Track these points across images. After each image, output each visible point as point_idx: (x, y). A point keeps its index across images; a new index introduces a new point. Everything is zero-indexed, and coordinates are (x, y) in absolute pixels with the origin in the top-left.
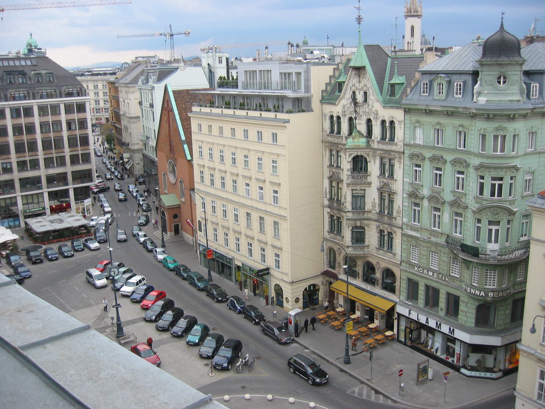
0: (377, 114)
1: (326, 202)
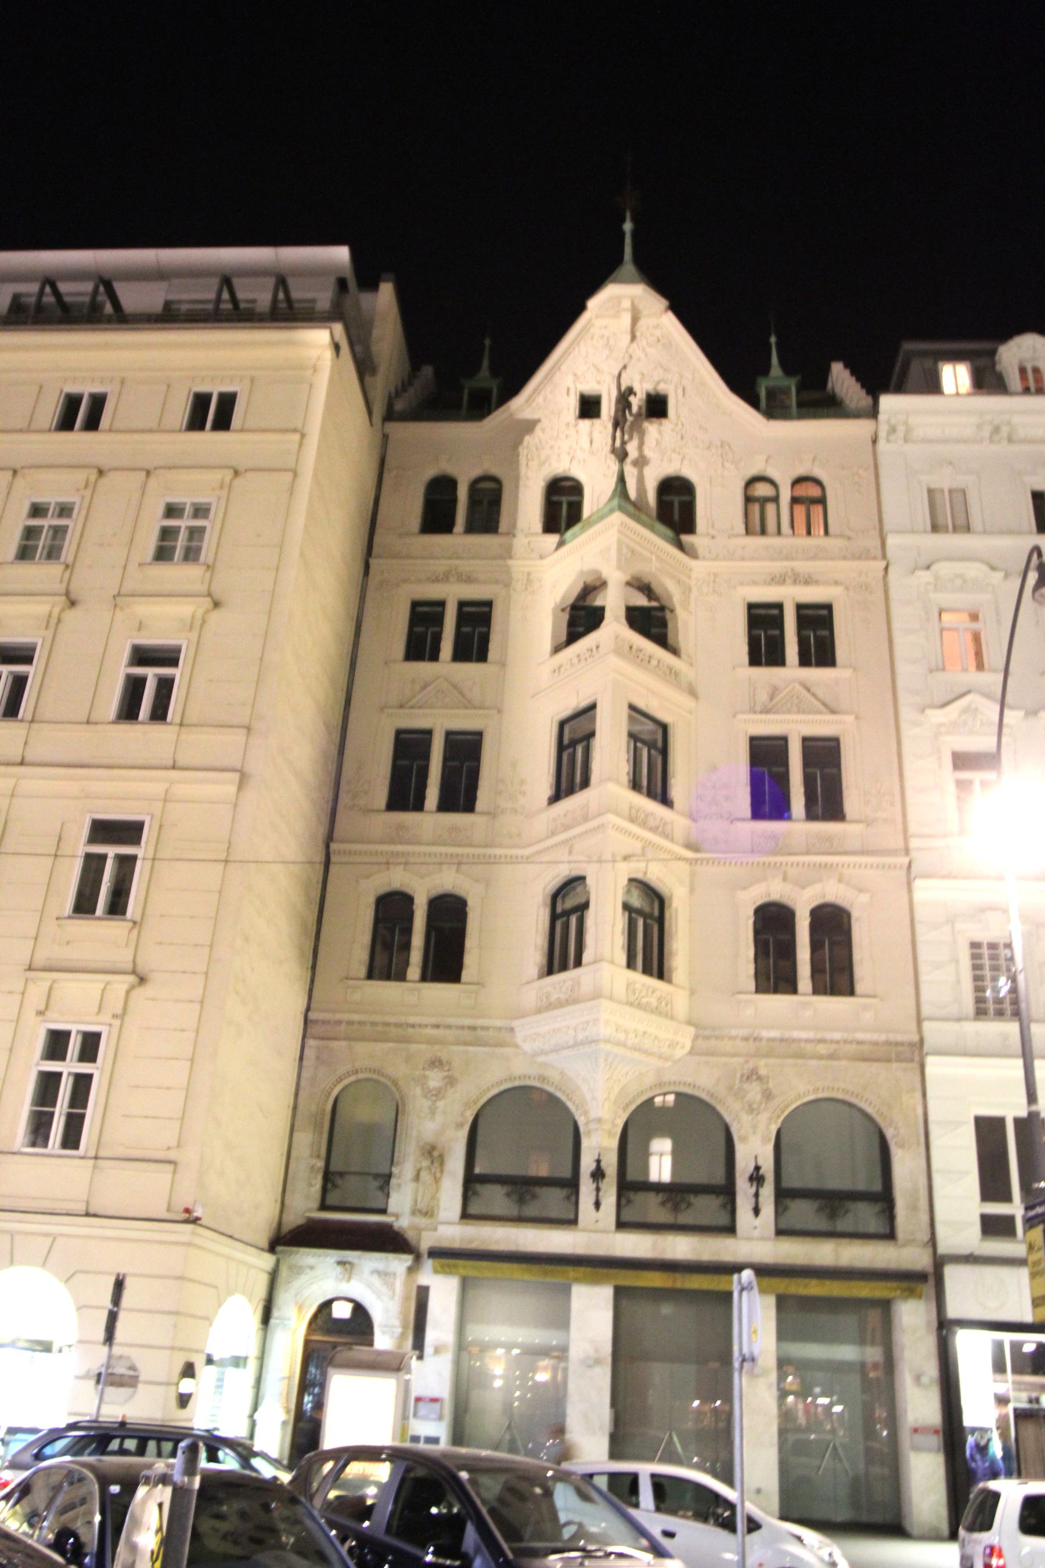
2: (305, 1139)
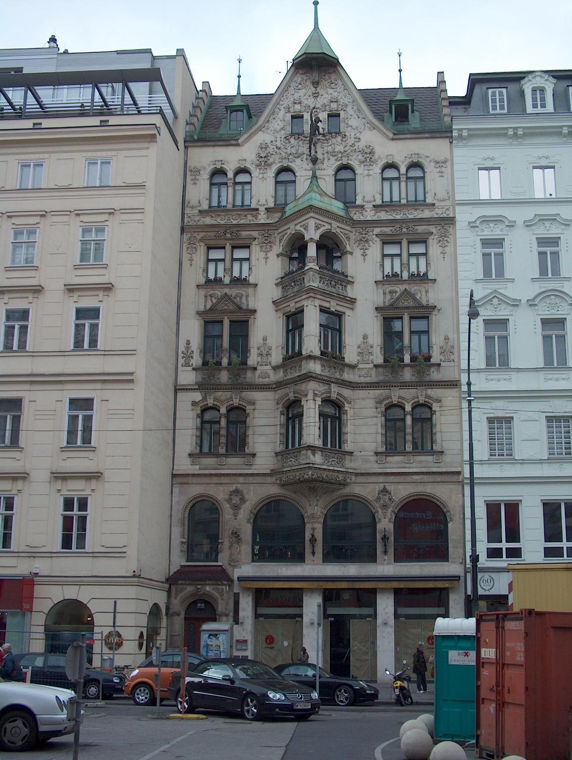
0: (372, 153)
1: (188, 377)
2: (177, 531)
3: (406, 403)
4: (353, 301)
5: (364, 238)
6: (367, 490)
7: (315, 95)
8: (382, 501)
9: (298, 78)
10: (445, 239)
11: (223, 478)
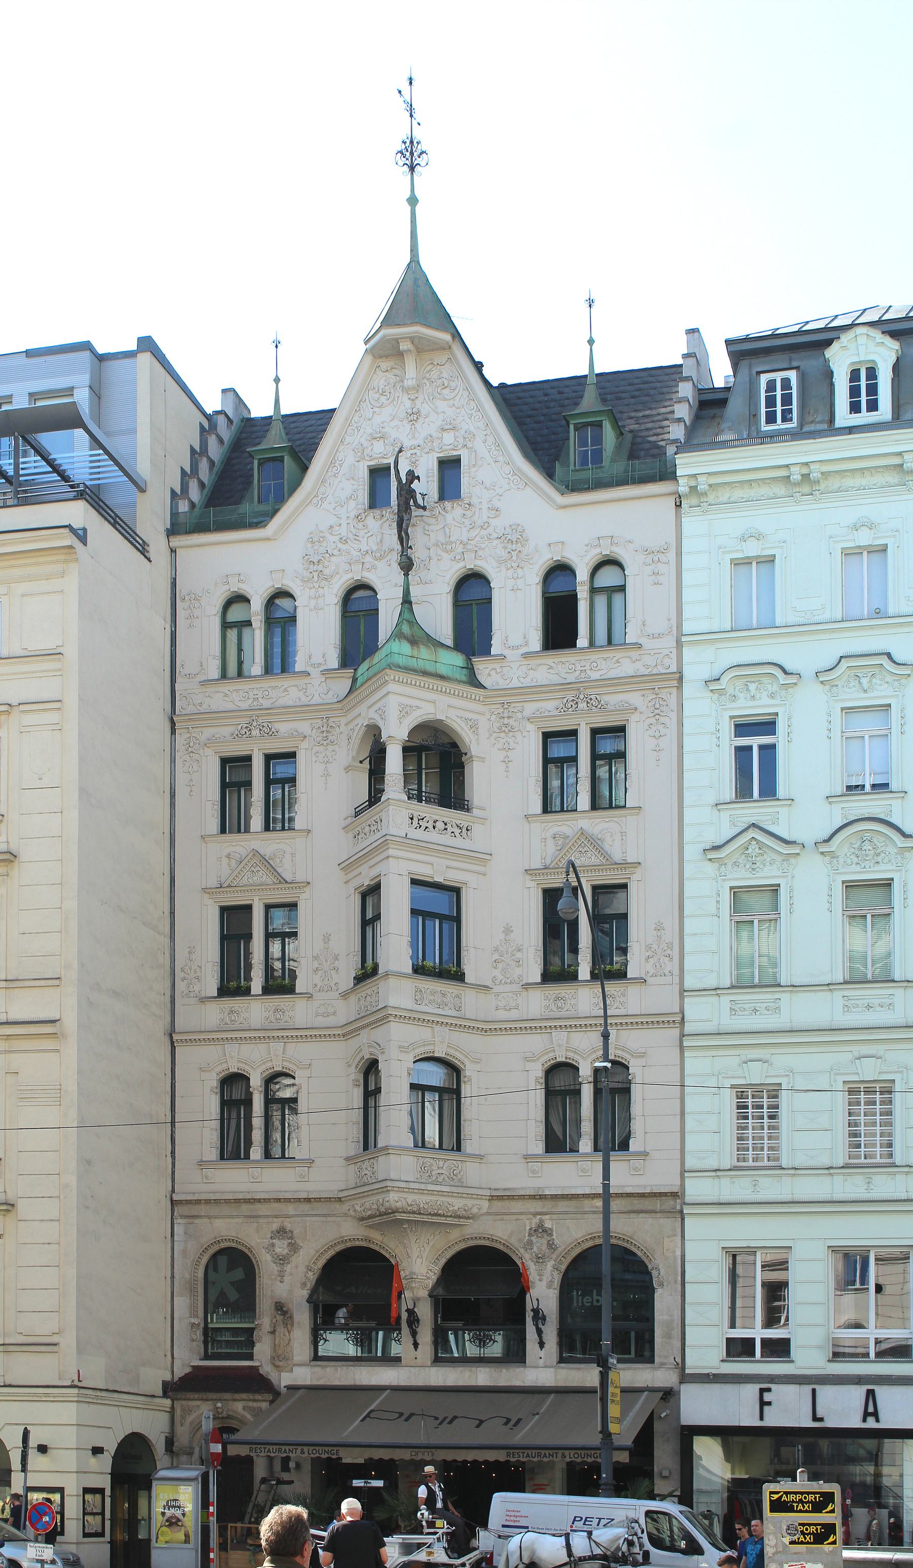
0: (522, 539)
2: (182, 1303)
3: (581, 1061)
4: (482, 858)
5: (506, 725)
6: (503, 1231)
7: (412, 418)
8: (535, 1249)
9: (380, 380)
10: (662, 719)
11: (258, 1206)
